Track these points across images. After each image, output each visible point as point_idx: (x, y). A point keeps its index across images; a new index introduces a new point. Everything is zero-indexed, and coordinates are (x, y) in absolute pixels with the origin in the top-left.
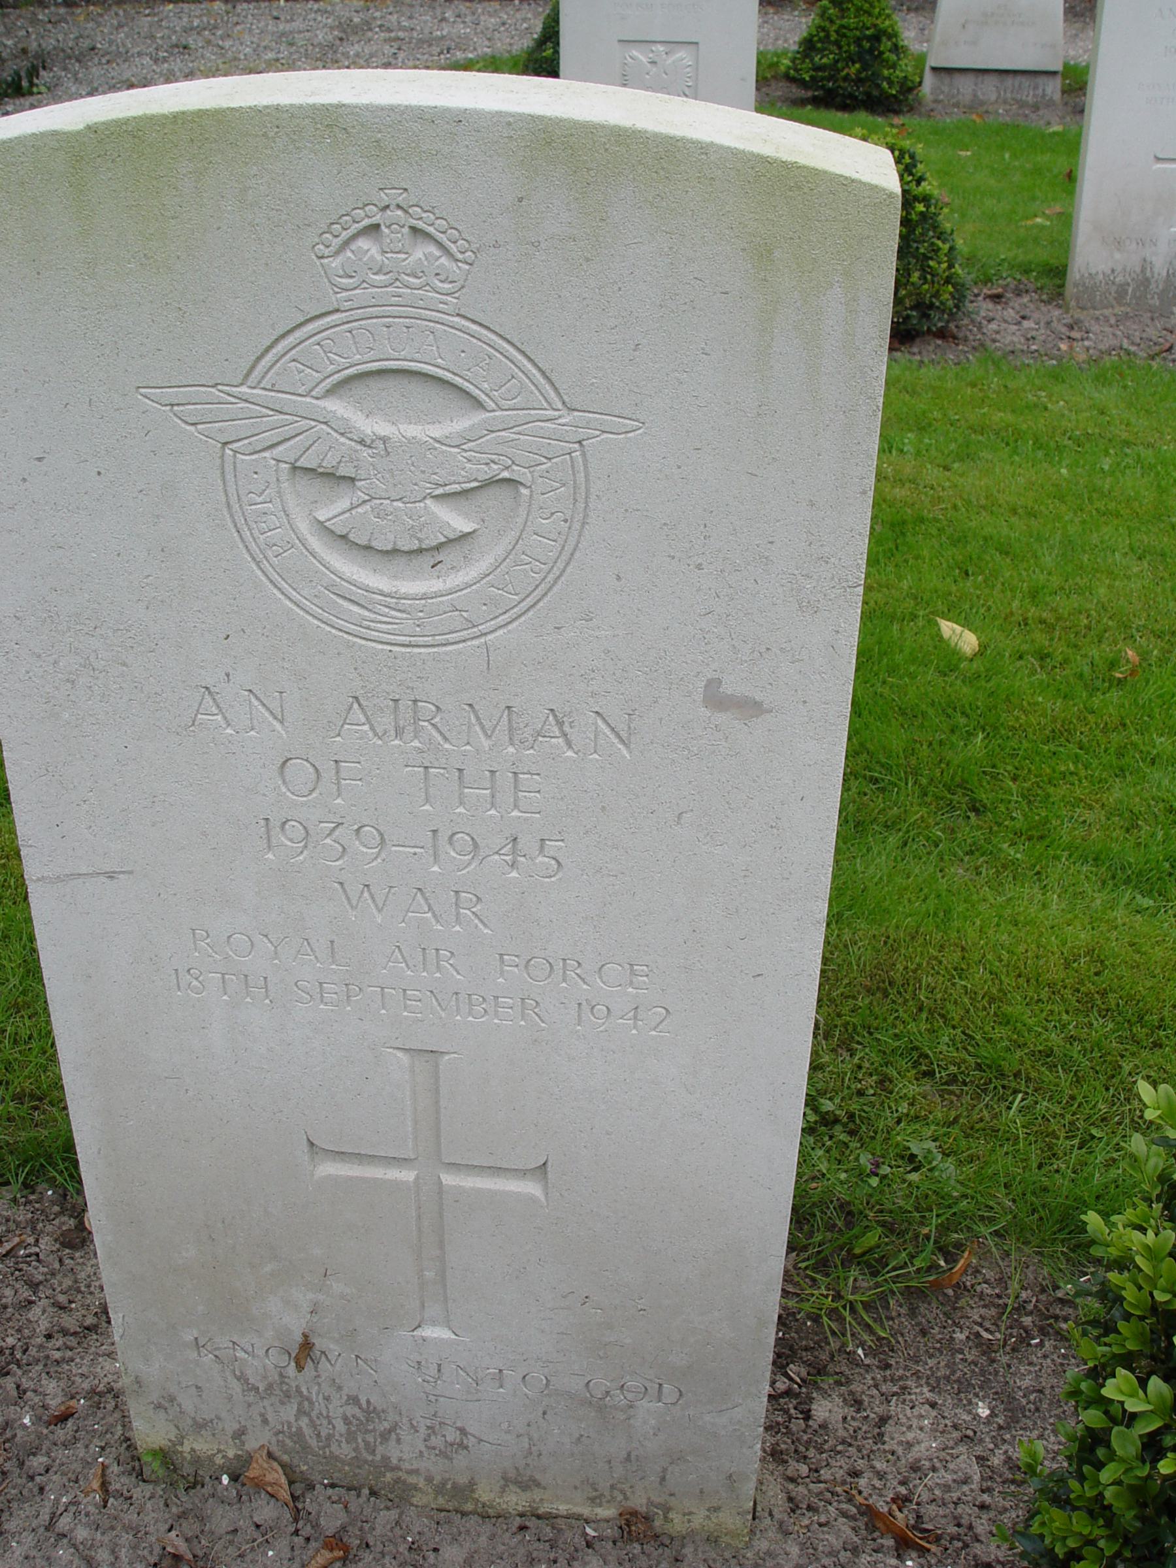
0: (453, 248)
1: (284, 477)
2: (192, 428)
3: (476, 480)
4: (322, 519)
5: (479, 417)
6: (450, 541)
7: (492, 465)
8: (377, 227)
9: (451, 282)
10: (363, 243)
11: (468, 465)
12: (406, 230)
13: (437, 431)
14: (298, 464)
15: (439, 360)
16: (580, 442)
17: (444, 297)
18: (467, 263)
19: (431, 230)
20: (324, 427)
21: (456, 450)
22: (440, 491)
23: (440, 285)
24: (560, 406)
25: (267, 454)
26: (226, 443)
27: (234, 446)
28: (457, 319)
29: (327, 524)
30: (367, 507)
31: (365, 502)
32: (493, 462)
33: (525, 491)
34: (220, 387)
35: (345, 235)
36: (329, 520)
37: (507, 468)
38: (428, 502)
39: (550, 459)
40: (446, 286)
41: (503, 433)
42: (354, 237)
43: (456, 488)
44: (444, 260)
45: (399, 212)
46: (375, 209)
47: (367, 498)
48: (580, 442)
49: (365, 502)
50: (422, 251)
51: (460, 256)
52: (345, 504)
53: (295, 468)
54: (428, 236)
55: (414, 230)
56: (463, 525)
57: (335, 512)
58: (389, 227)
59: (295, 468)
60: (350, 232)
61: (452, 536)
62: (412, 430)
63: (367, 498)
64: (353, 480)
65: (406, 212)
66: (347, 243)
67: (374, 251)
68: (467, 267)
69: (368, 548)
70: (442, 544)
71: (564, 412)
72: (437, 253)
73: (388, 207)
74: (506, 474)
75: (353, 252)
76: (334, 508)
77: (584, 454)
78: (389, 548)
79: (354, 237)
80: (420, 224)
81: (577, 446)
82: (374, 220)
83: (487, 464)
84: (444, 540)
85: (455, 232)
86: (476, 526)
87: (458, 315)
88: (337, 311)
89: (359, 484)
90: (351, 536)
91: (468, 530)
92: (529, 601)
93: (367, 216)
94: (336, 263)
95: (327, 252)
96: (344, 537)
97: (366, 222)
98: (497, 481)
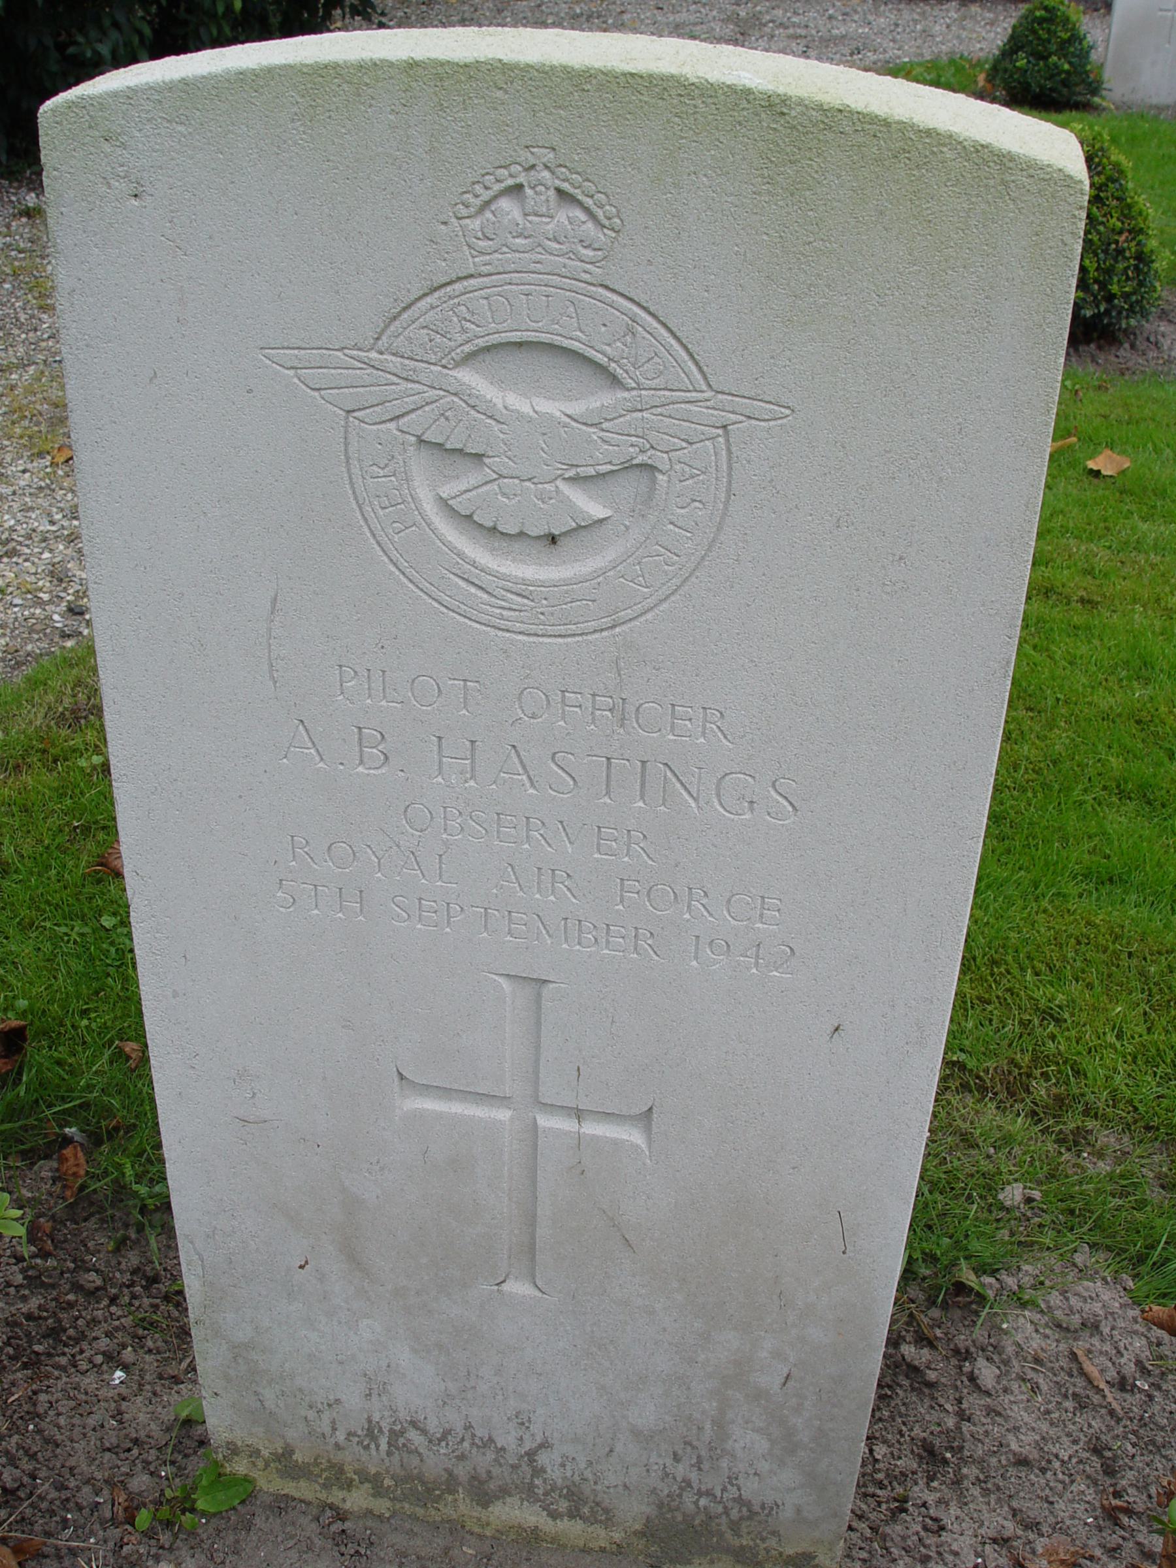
0: (600, 213)
2: (316, 394)
3: (610, 463)
4: (444, 496)
8: (519, 187)
9: (595, 250)
10: (504, 203)
12: (552, 192)
15: (578, 333)
16: (724, 427)
17: (588, 266)
18: (613, 229)
19: (577, 193)
20: (456, 399)
22: (571, 473)
24: (704, 388)
25: (389, 425)
26: (348, 412)
28: (600, 290)
29: (450, 502)
30: (494, 486)
33: (660, 477)
34: (346, 351)
35: (486, 195)
38: (559, 483)
40: (591, 253)
43: (591, 471)
44: (590, 225)
46: (520, 168)
47: (495, 476)
48: (724, 427)
50: (565, 215)
51: (606, 223)
53: (421, 441)
55: (559, 191)
56: (597, 511)
58: (533, 188)
59: (421, 441)
60: (490, 193)
62: (546, 406)
63: (495, 476)
64: (479, 457)
65: (553, 173)
66: (487, 203)
67: (517, 214)
68: (614, 235)
70: (574, 530)
72: (583, 217)
73: (533, 167)
75: (493, 212)
77: (727, 441)
78: (513, 531)
80: (565, 186)
81: (720, 431)
82: (518, 181)
84: (574, 525)
85: (603, 196)
87: (601, 285)
89: (487, 461)
90: (475, 518)
93: (511, 176)
94: (475, 224)
95: (464, 212)
97: (510, 182)
98: (633, 465)
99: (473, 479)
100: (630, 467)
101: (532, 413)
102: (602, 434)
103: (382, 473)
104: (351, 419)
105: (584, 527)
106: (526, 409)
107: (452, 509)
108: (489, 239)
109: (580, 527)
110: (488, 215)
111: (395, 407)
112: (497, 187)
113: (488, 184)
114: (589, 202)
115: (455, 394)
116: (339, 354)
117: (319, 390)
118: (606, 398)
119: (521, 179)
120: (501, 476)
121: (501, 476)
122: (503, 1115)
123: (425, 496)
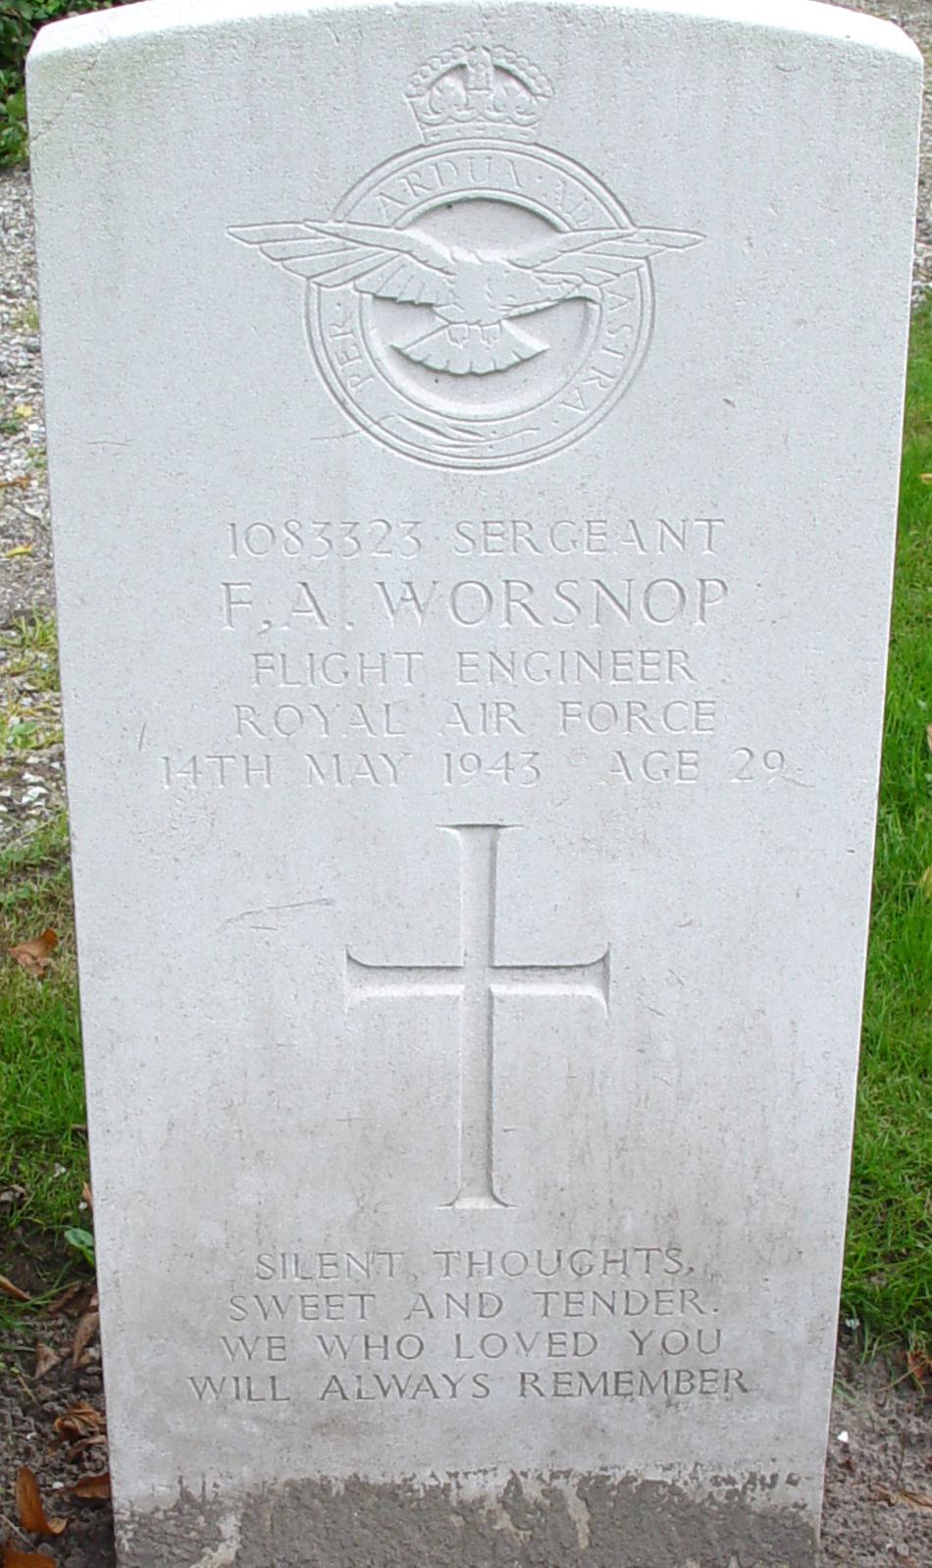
0: (532, 83)
3: (548, 300)
5: (552, 240)
7: (564, 285)
8: (462, 67)
10: (449, 81)
11: (542, 286)
12: (491, 70)
14: (381, 294)
15: (517, 188)
16: (646, 258)
17: (525, 128)
18: (544, 96)
20: (406, 256)
22: (515, 312)
23: (519, 116)
25: (350, 285)
26: (308, 278)
27: (317, 280)
29: (407, 351)
31: (444, 327)
32: (567, 281)
33: (596, 307)
35: (433, 75)
36: (408, 346)
39: (617, 275)
43: (532, 308)
44: (524, 94)
47: (445, 323)
48: (646, 258)
49: (444, 327)
50: (501, 87)
53: (376, 298)
54: (508, 73)
55: (498, 68)
56: (538, 345)
59: (376, 298)
61: (526, 356)
63: (445, 323)
64: (429, 306)
70: (516, 365)
71: (632, 229)
74: (577, 293)
76: (414, 333)
80: (503, 63)
81: (643, 262)
83: (559, 283)
84: (516, 359)
86: (546, 347)
87: (536, 144)
89: (438, 310)
91: (539, 350)
92: (598, 415)
93: (454, 57)
95: (414, 91)
97: (454, 62)
101: (477, 262)
102: (538, 275)
103: (340, 331)
104: (312, 285)
105: (528, 360)
106: (470, 258)
107: (407, 358)
108: (436, 113)
109: (524, 361)
111: (353, 269)
112: (443, 68)
113: (435, 65)
114: (521, 74)
115: (409, 253)
116: (302, 227)
117: (282, 259)
119: (464, 60)
120: (451, 323)
121: (451, 323)
122: (453, 989)
123: (380, 349)
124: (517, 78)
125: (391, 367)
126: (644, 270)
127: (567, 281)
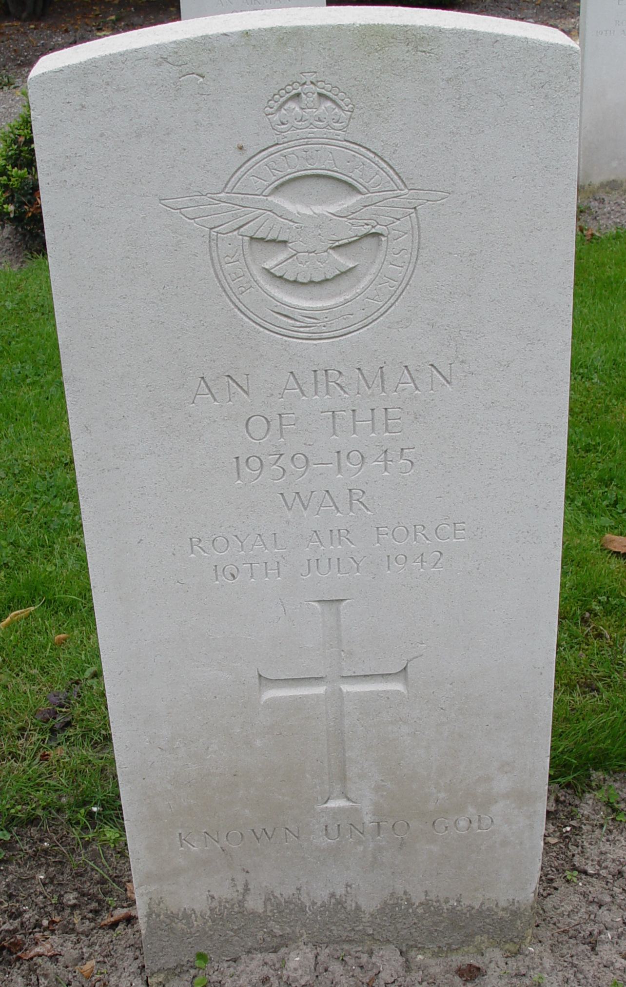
0: (342, 104)
1: (246, 244)
4: (267, 267)
6: (343, 273)
10: (291, 105)
13: (333, 209)
16: (415, 208)
21: (345, 219)
22: (337, 244)
24: (403, 187)
25: (235, 233)
27: (215, 230)
29: (272, 271)
33: (383, 239)
37: (373, 227)
38: (330, 251)
41: (373, 207)
42: (285, 102)
44: (337, 110)
45: (312, 86)
48: (415, 208)
52: (282, 257)
54: (327, 98)
55: (320, 95)
57: (275, 263)
59: (251, 238)
60: (284, 99)
61: (343, 270)
62: (318, 209)
64: (285, 242)
69: (295, 282)
71: (406, 191)
72: (334, 107)
73: (304, 84)
74: (373, 231)
76: (275, 260)
79: (285, 102)
84: (338, 272)
88: (277, 144)
91: (351, 266)
93: (294, 89)
94: (276, 118)
95: (271, 111)
96: (280, 277)
99: (282, 257)
100: (367, 235)
106: (308, 212)
107: (272, 273)
110: (283, 111)
112: (288, 95)
114: (334, 97)
118: (352, 201)
124: (334, 102)
125: (262, 280)
126: (414, 215)
127: (367, 225)
